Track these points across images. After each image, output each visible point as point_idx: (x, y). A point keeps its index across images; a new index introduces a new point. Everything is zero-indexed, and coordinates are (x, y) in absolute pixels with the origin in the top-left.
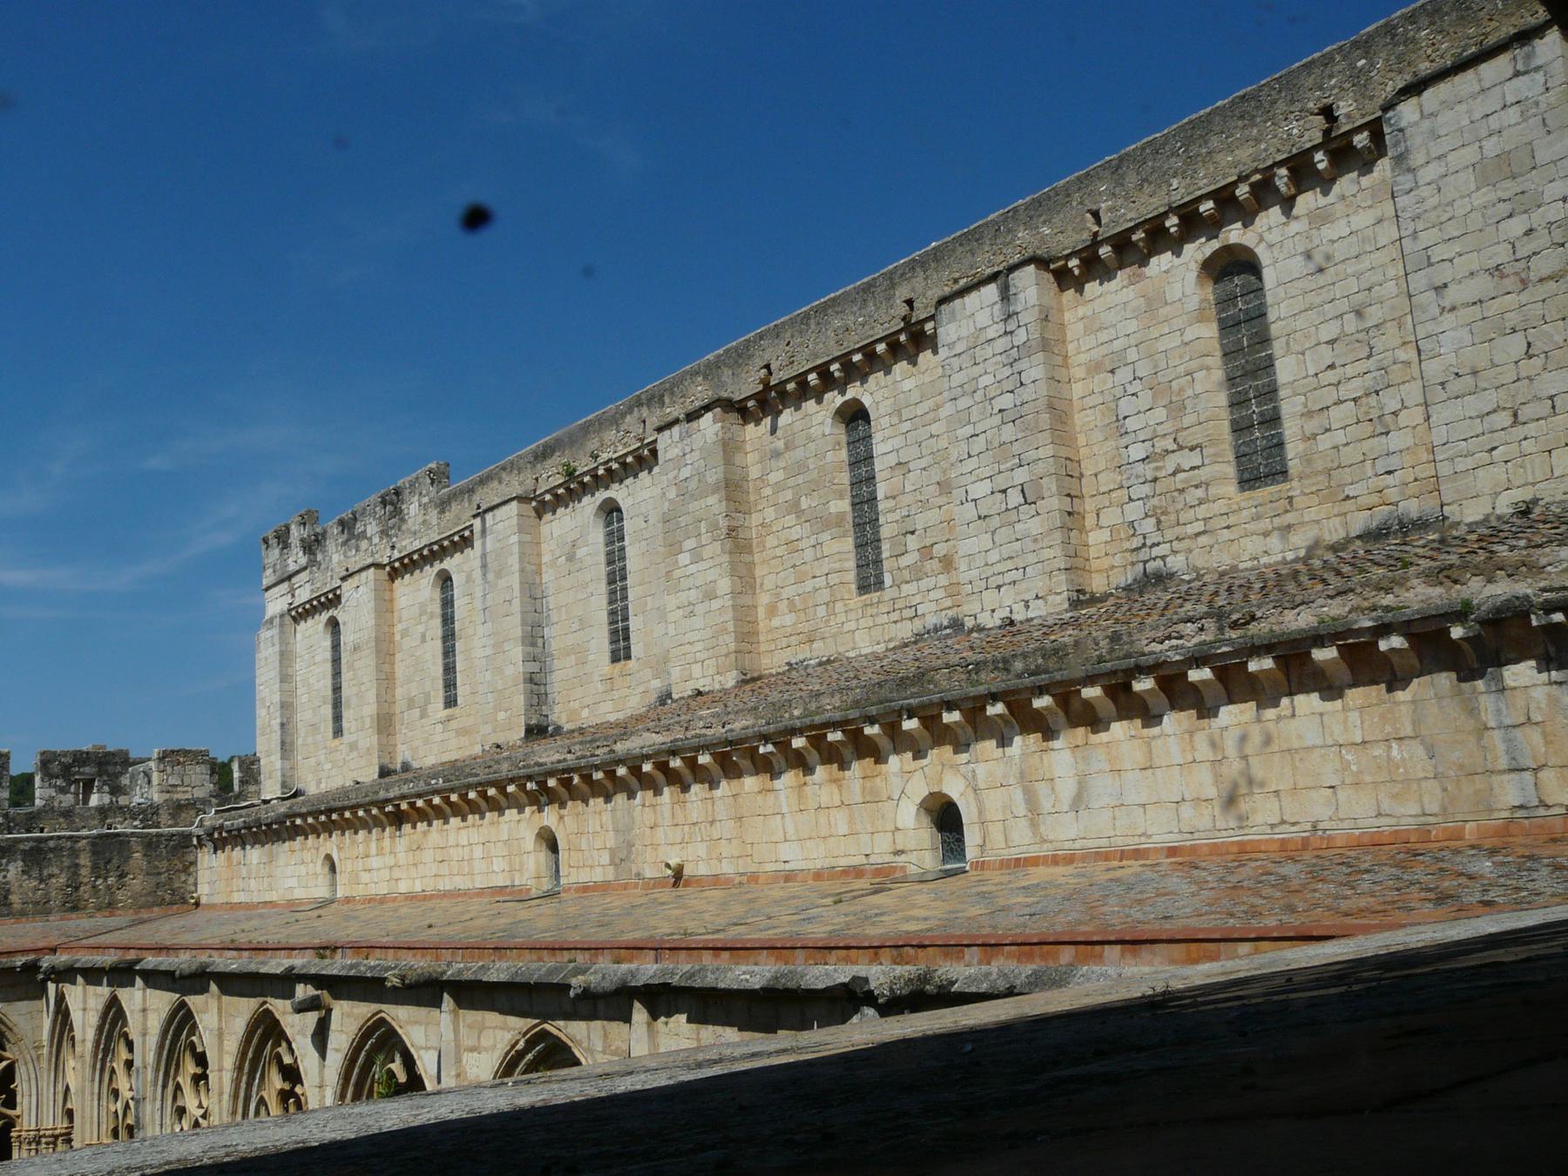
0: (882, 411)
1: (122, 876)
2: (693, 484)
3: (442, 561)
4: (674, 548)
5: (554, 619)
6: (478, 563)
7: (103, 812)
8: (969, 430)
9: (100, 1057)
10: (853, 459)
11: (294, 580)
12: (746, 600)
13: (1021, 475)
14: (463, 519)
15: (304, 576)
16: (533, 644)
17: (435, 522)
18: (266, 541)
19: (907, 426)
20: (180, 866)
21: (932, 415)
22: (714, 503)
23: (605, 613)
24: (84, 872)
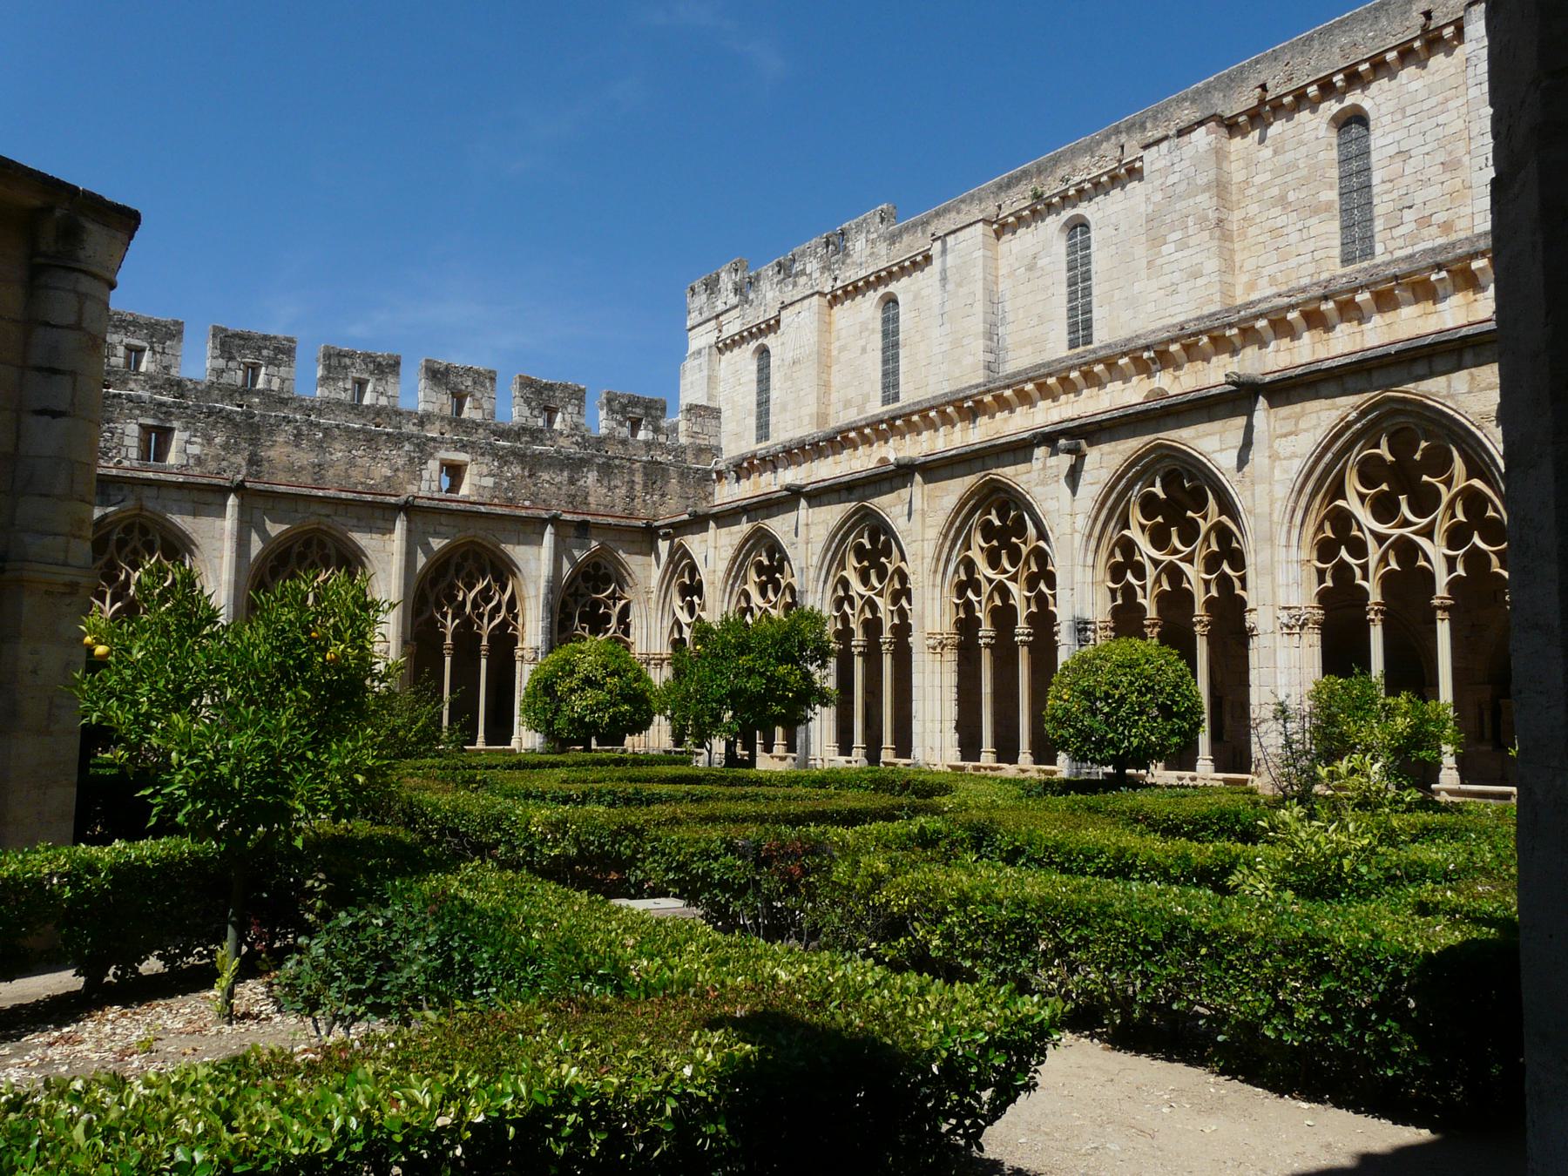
1: (663, 496)
2: (1182, 187)
3: (887, 285)
4: (1156, 241)
5: (1010, 317)
6: (938, 277)
7: (648, 445)
10: (1343, 158)
11: (721, 318)
12: (1228, 278)
14: (916, 246)
16: (991, 339)
17: (884, 252)
18: (692, 289)
20: (702, 495)
21: (1439, 108)
22: (1205, 201)
23: (1065, 310)
24: (638, 487)
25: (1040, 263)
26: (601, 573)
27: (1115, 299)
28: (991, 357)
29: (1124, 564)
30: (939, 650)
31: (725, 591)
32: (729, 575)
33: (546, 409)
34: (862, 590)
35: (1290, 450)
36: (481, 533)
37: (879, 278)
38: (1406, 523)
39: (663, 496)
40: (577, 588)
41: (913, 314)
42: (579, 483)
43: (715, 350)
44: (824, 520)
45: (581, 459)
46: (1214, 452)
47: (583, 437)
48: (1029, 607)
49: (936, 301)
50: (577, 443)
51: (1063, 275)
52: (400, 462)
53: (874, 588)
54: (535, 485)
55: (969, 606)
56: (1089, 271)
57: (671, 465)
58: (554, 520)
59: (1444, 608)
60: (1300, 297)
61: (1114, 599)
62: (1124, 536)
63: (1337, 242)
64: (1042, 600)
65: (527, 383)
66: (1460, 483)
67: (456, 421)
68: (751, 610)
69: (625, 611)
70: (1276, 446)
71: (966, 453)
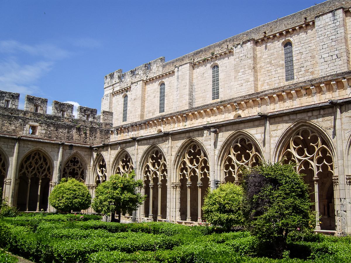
0: (296, 41)
1: (95, 137)
4: (237, 72)
6: (176, 78)
7: (91, 122)
8: (323, 43)
9: (114, 165)
10: (286, 53)
12: (256, 83)
13: (336, 52)
15: (118, 84)
16: (191, 96)
17: (161, 70)
18: (106, 77)
19: (303, 45)
20: (107, 137)
22: (250, 61)
23: (212, 89)
24: (88, 135)
25: (205, 75)
26: (76, 160)
27: (226, 87)
28: (191, 101)
29: (229, 164)
30: (175, 188)
31: (112, 167)
32: (114, 162)
33: (62, 111)
34: (153, 169)
35: (275, 135)
36: (41, 147)
37: (159, 77)
38: (306, 156)
40: (69, 165)
41: (169, 88)
42: (71, 133)
44: (142, 149)
45: (71, 126)
46: (255, 134)
47: (72, 119)
48: (201, 176)
49: (176, 84)
50: (71, 121)
51: (211, 79)
52: (18, 125)
53: (156, 169)
54: (57, 133)
55: (184, 175)
56: (218, 78)
57: (98, 128)
58: (63, 144)
59: (317, 181)
60: (277, 90)
61: (226, 175)
62: (229, 157)
63: (285, 75)
64: (205, 174)
65: (56, 103)
66: (320, 146)
67: (35, 114)
70: (271, 133)
71: (184, 131)
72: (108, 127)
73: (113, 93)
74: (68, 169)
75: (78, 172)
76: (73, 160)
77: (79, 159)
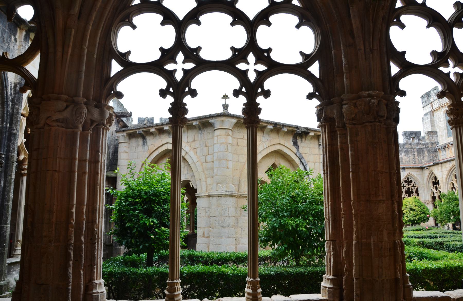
1: (423, 157)
7: (417, 144)
9: (447, 180)
11: (432, 103)
26: (409, 180)
32: (447, 178)
39: (423, 157)
43: (431, 113)
57: (425, 149)
68: (455, 188)
69: (417, 191)
72: (434, 145)
73: (433, 111)
74: (403, 188)
75: (413, 190)
76: (407, 180)
77: (412, 179)
